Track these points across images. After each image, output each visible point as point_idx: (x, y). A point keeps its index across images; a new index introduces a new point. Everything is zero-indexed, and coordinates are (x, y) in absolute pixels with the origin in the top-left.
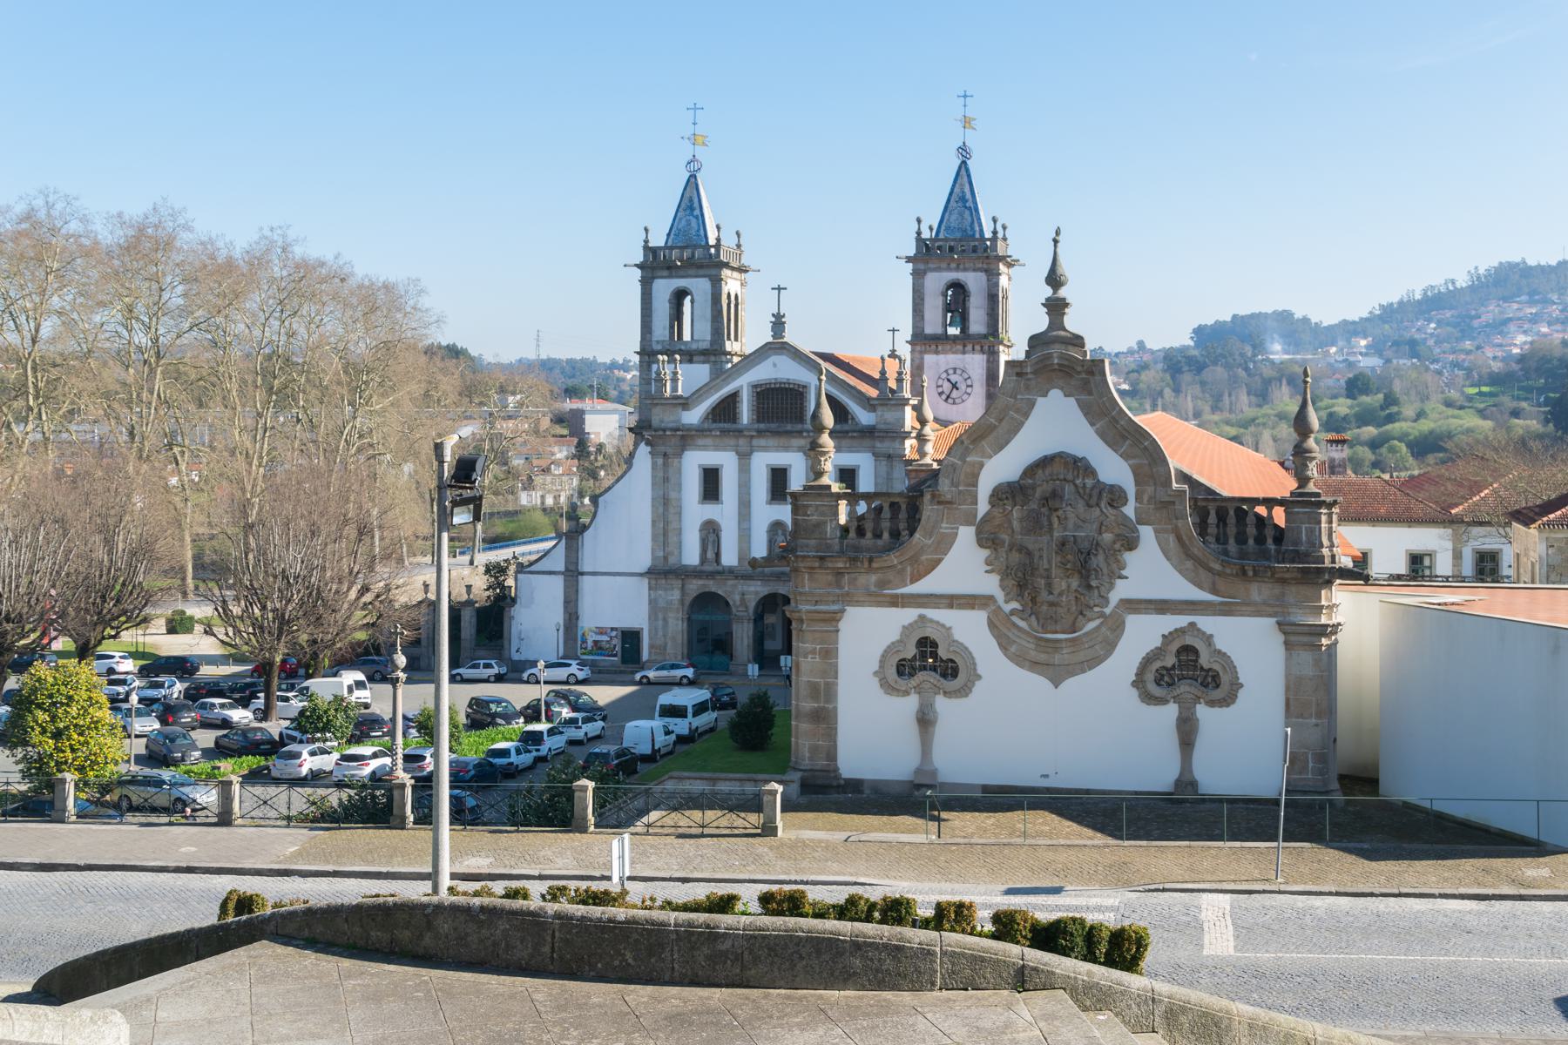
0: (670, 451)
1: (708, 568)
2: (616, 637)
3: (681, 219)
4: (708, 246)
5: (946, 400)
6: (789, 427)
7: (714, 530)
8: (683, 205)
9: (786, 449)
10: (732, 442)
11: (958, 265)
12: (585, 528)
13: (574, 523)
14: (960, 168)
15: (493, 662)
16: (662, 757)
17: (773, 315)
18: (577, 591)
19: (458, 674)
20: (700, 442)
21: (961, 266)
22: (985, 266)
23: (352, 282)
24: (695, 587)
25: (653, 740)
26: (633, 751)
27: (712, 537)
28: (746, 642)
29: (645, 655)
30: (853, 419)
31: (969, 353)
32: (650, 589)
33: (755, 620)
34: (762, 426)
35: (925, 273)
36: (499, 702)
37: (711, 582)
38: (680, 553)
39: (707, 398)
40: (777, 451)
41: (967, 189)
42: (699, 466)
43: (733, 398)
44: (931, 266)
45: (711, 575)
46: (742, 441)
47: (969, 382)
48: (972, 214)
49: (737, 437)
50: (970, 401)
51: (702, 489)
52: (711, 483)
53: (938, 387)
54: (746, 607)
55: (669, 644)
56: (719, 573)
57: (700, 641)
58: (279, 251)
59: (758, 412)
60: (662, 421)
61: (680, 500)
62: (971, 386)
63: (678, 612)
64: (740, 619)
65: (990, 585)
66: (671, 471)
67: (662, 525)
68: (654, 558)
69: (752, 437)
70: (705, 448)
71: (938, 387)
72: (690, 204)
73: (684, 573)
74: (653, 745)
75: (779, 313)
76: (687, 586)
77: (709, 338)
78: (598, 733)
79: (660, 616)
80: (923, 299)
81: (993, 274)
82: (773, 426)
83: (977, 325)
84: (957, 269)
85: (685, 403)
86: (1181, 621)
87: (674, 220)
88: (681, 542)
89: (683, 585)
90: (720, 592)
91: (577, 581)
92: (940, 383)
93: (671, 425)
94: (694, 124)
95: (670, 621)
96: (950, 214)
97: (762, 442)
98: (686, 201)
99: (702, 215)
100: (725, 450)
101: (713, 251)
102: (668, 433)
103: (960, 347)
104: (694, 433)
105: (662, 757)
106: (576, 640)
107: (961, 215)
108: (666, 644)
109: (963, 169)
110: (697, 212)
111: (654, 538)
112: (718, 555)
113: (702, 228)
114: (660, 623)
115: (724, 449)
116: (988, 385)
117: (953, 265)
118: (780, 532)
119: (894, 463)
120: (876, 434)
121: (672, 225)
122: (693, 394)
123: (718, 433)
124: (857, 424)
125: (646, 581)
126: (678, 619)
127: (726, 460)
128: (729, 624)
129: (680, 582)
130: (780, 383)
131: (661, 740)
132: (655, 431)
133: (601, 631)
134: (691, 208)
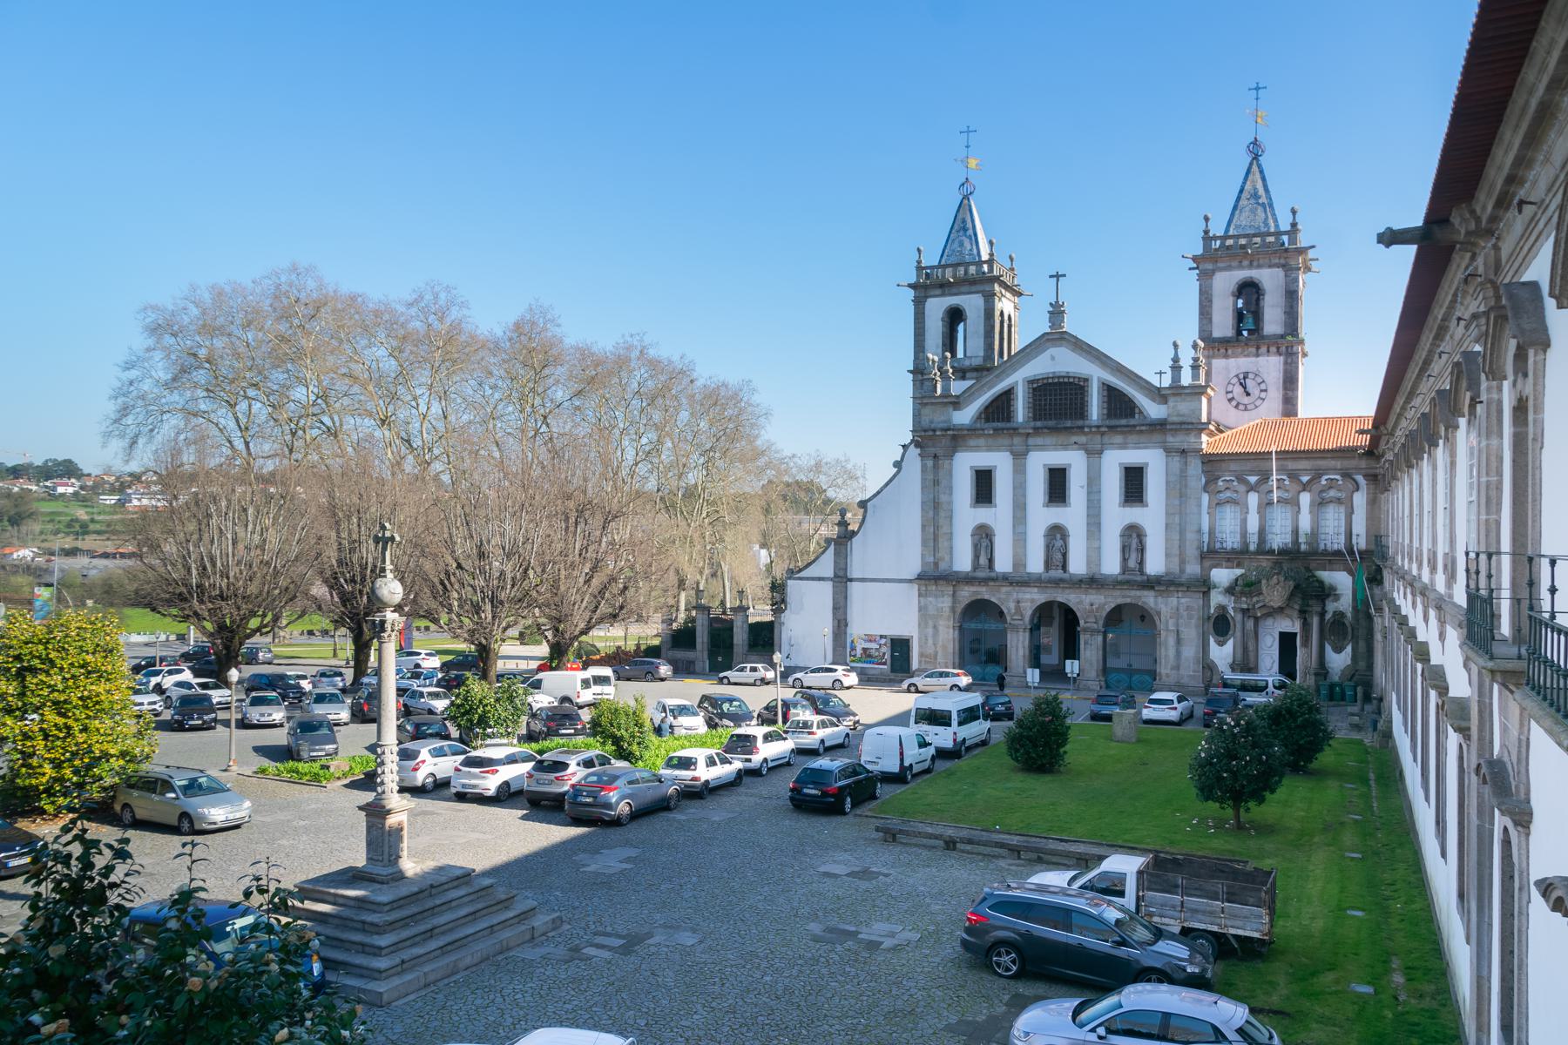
0: (940, 452)
1: (980, 574)
4: (980, 263)
5: (1236, 407)
6: (1069, 424)
7: (987, 535)
8: (956, 227)
9: (1065, 447)
10: (1006, 441)
11: (1251, 262)
12: (854, 533)
13: (843, 528)
14: (1251, 164)
15: (759, 666)
16: (914, 776)
17: (1051, 304)
18: (846, 598)
20: (972, 442)
21: (1255, 264)
22: (1282, 261)
24: (967, 594)
25: (902, 754)
26: (869, 767)
27: (985, 543)
28: (1021, 652)
29: (915, 665)
30: (1141, 412)
32: (920, 595)
33: (1031, 629)
34: (1039, 424)
35: (1213, 272)
37: (984, 589)
38: (951, 558)
39: (981, 396)
40: (1056, 450)
41: (1260, 185)
42: (971, 468)
43: (1008, 395)
44: (1221, 265)
45: (984, 581)
46: (1017, 440)
47: (1263, 386)
48: (1265, 212)
49: (1011, 436)
50: (1264, 407)
51: (974, 492)
52: (984, 486)
53: (1227, 393)
55: (940, 654)
56: (993, 579)
57: (973, 651)
60: (931, 422)
61: (950, 503)
62: (1266, 391)
63: (948, 620)
64: (1015, 628)
66: (941, 473)
68: (924, 563)
70: (977, 448)
71: (1227, 393)
72: (961, 226)
74: (902, 760)
75: (1057, 302)
76: (958, 593)
77: (982, 354)
78: (840, 741)
80: (1211, 301)
81: (1292, 269)
82: (1051, 423)
83: (1272, 323)
84: (1251, 266)
85: (957, 403)
87: (947, 241)
88: (952, 548)
89: (954, 592)
90: (993, 600)
92: (1230, 389)
94: (967, 147)
95: (941, 628)
96: (1241, 212)
97: (1039, 440)
98: (959, 221)
99: (975, 235)
100: (999, 450)
101: (985, 267)
102: (938, 433)
103: (1253, 350)
104: (966, 432)
105: (914, 776)
106: (845, 647)
107: (1253, 211)
109: (1255, 167)
110: (970, 232)
111: (924, 543)
112: (991, 561)
113: (974, 247)
114: (930, 631)
115: (998, 449)
116: (1285, 388)
117: (1246, 263)
118: (1058, 536)
119: (1189, 459)
120: (1168, 427)
121: (945, 246)
123: (991, 432)
126: (948, 627)
127: (999, 462)
128: (1003, 633)
129: (951, 588)
130: (1059, 377)
131: (913, 754)
132: (925, 431)
133: (870, 639)
134: (965, 229)
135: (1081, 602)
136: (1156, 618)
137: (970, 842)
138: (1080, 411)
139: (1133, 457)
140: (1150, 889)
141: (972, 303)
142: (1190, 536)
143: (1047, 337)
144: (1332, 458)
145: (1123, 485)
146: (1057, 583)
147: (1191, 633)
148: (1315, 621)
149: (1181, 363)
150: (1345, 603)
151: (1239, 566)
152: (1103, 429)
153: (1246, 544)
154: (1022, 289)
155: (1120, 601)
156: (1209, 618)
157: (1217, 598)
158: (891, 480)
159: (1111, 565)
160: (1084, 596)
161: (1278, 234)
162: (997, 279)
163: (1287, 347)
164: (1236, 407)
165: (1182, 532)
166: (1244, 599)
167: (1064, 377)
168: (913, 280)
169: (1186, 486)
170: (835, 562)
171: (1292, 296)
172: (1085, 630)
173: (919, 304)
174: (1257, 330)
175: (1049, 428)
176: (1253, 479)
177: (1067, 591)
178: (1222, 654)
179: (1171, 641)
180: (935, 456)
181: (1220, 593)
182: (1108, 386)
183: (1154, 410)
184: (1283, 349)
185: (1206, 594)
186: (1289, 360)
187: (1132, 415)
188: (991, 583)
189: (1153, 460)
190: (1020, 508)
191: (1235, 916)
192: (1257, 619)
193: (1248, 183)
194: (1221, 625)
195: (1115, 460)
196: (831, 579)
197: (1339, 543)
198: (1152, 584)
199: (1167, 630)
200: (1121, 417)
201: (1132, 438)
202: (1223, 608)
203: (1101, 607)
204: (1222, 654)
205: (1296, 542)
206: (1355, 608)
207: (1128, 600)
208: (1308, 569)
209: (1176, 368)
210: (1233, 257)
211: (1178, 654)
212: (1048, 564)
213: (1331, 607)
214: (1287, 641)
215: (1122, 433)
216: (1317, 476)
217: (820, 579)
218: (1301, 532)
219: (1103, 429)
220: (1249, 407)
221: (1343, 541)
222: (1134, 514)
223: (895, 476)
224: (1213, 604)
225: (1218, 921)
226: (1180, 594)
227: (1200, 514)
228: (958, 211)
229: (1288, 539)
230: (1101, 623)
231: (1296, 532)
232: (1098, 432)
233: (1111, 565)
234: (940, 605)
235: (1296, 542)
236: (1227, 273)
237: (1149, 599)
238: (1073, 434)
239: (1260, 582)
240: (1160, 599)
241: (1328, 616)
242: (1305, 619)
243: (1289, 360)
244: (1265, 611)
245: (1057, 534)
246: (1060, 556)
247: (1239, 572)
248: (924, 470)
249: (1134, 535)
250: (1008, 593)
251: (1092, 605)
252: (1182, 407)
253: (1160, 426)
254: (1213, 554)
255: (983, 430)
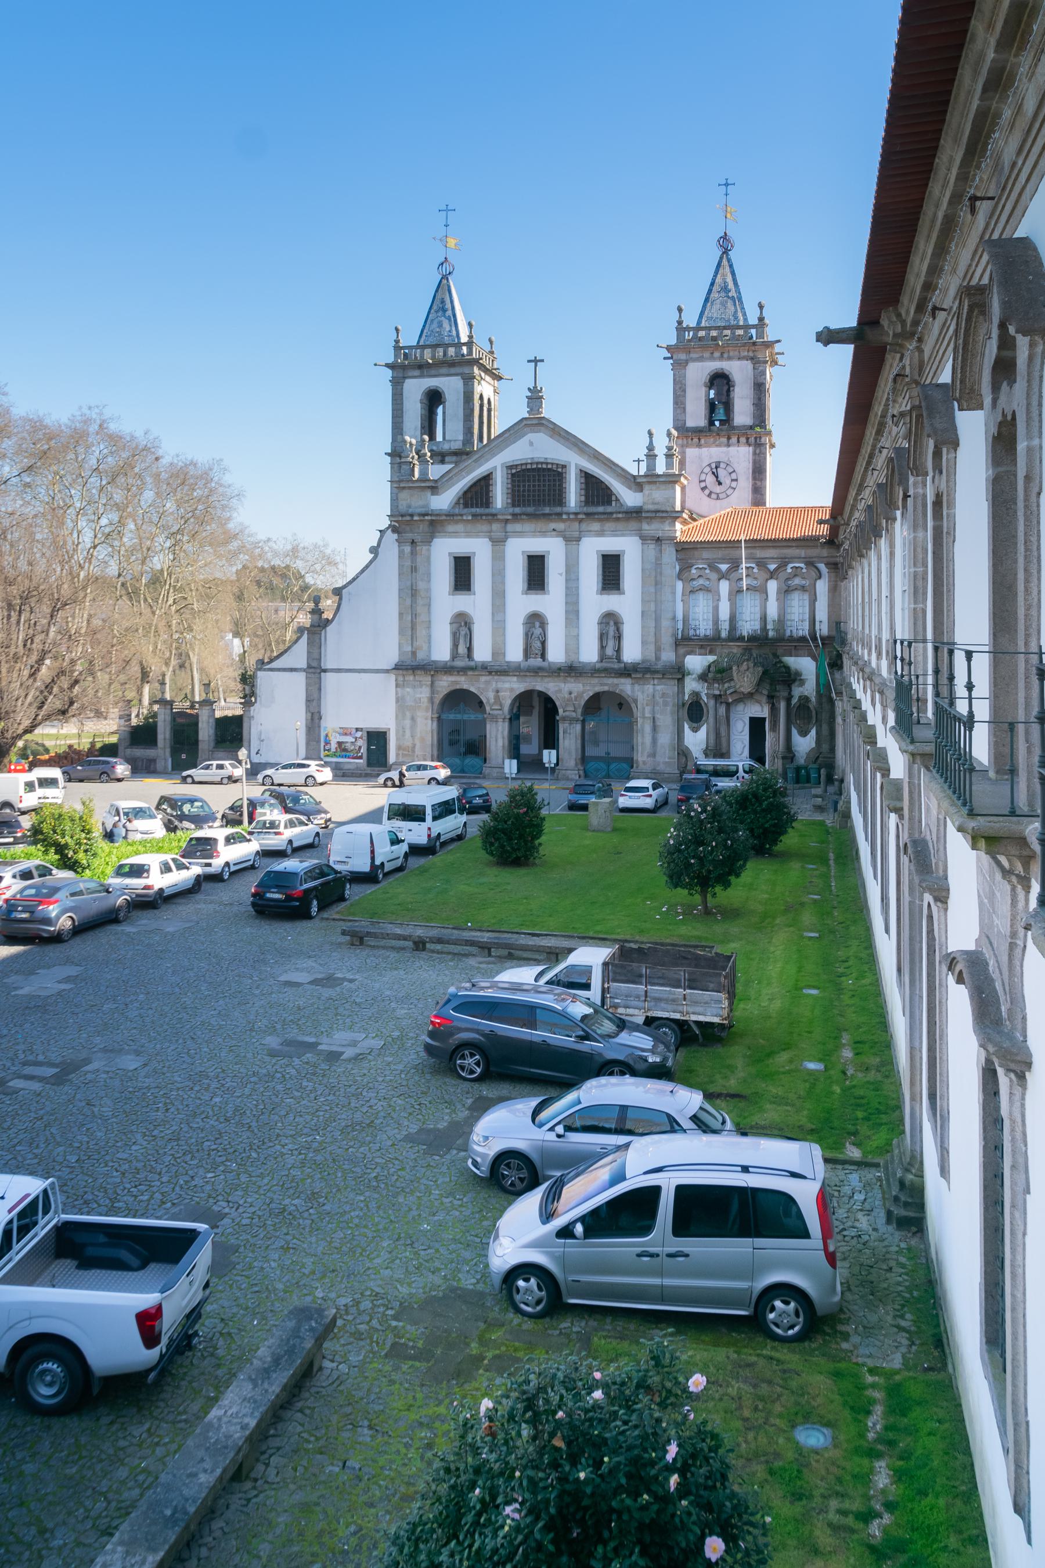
0: (418, 538)
1: (459, 663)
2: (361, 738)
3: (432, 321)
4: (459, 345)
5: (709, 496)
6: (547, 510)
7: (466, 623)
8: (435, 307)
9: (543, 534)
10: (485, 527)
11: (722, 354)
12: (328, 622)
13: (316, 617)
14: (721, 258)
16: (386, 875)
17: (529, 389)
18: (320, 689)
19: (189, 776)
20: (450, 528)
21: (726, 355)
22: (751, 354)
23: (165, 461)
24: (445, 684)
25: (373, 852)
26: (338, 867)
27: (464, 631)
28: (500, 743)
29: (392, 758)
30: (617, 500)
31: (734, 445)
32: (397, 686)
33: (510, 719)
34: (517, 510)
35: (687, 362)
36: (192, 801)
37: (463, 679)
38: (430, 647)
40: (534, 536)
41: (729, 279)
42: (450, 554)
44: (693, 355)
45: (463, 670)
46: (495, 526)
47: (734, 476)
48: (735, 305)
49: (490, 522)
50: (736, 494)
51: (453, 579)
54: (501, 705)
56: (472, 669)
57: (452, 743)
58: (97, 427)
59: (513, 496)
60: (409, 507)
61: (428, 590)
62: (736, 480)
63: (427, 711)
64: (494, 719)
66: (419, 559)
67: (410, 618)
68: (401, 653)
69: (507, 521)
70: (455, 534)
73: (432, 669)
74: (373, 859)
75: (535, 387)
76: (437, 683)
77: (461, 438)
78: (310, 840)
79: (408, 714)
80: (684, 391)
81: (759, 362)
82: (530, 510)
83: (742, 414)
84: (721, 358)
85: (434, 488)
88: (430, 636)
89: (432, 683)
90: (472, 689)
91: (320, 678)
92: (703, 477)
93: (419, 510)
94: (446, 226)
95: (419, 720)
97: (518, 527)
98: (437, 302)
99: (454, 316)
100: (478, 537)
101: (465, 350)
102: (416, 518)
103: (724, 440)
104: (444, 518)
105: (386, 875)
106: (319, 741)
107: (724, 305)
108: (414, 746)
109: (725, 262)
110: (449, 313)
112: (470, 649)
114: (408, 722)
116: (754, 478)
117: (717, 354)
118: (537, 624)
121: (424, 326)
122: (443, 476)
123: (470, 518)
124: (622, 505)
125: (392, 677)
126: (426, 719)
128: (483, 723)
129: (429, 678)
130: (537, 463)
131: (385, 852)
132: (402, 516)
133: (345, 732)
134: (444, 310)
135: (560, 691)
136: (633, 705)
137: (440, 941)
138: (558, 497)
139: (611, 544)
140: (615, 980)
141: (450, 385)
142: (665, 623)
143: (525, 422)
144: (797, 547)
145: (601, 572)
146: (536, 671)
147: (666, 720)
148: (782, 706)
149: (656, 452)
150: (809, 688)
151: (711, 653)
152: (580, 516)
153: (718, 631)
154: (502, 372)
155: (598, 689)
156: (684, 705)
157: (691, 685)
158: (367, 567)
159: (589, 654)
160: (562, 685)
161: (747, 327)
162: (476, 362)
163: (756, 438)
164: (709, 496)
165: (657, 620)
166: (716, 685)
167: (542, 463)
168: (391, 359)
169: (661, 573)
170: (309, 652)
171: (760, 389)
172: (564, 719)
173: (397, 384)
174: (727, 421)
175: (527, 515)
176: (724, 567)
177: (546, 680)
178: (696, 740)
179: (648, 728)
180: (413, 542)
181: (694, 679)
182: (586, 473)
183: (630, 498)
184: (752, 440)
185: (681, 681)
186: (758, 451)
187: (609, 503)
188: (470, 673)
190: (499, 595)
191: (696, 1003)
192: (728, 705)
193: (719, 276)
194: (695, 712)
196: (304, 670)
197: (804, 630)
198: (628, 671)
199: (644, 717)
200: (598, 504)
201: (609, 525)
202: (696, 694)
203: (580, 695)
204: (696, 740)
205: (764, 628)
206: (818, 691)
207: (606, 688)
208: (775, 655)
209: (651, 456)
210: (704, 348)
211: (654, 741)
212: (527, 652)
213: (797, 692)
214: (757, 726)
215: (600, 520)
216: (783, 565)
217: (292, 670)
218: (769, 619)
219: (580, 516)
220: (721, 496)
221: (807, 628)
222: (612, 602)
223: (371, 562)
224: (688, 690)
225: (680, 1008)
226: (656, 682)
227: (674, 601)
228: (437, 291)
229: (757, 626)
230: (580, 711)
231: (764, 619)
232: (576, 519)
233: (589, 654)
234: (418, 696)
235: (764, 628)
236: (700, 364)
237: (626, 687)
238: (551, 521)
239: (731, 668)
240: (637, 687)
241: (794, 701)
242: (773, 704)
243: (758, 451)
244: (736, 697)
245: (536, 621)
246: (539, 644)
247: (711, 658)
248: (401, 555)
249: (612, 623)
250: (487, 683)
251: (570, 693)
252: (654, 496)
253: (636, 514)
254: (686, 642)
255: (462, 515)
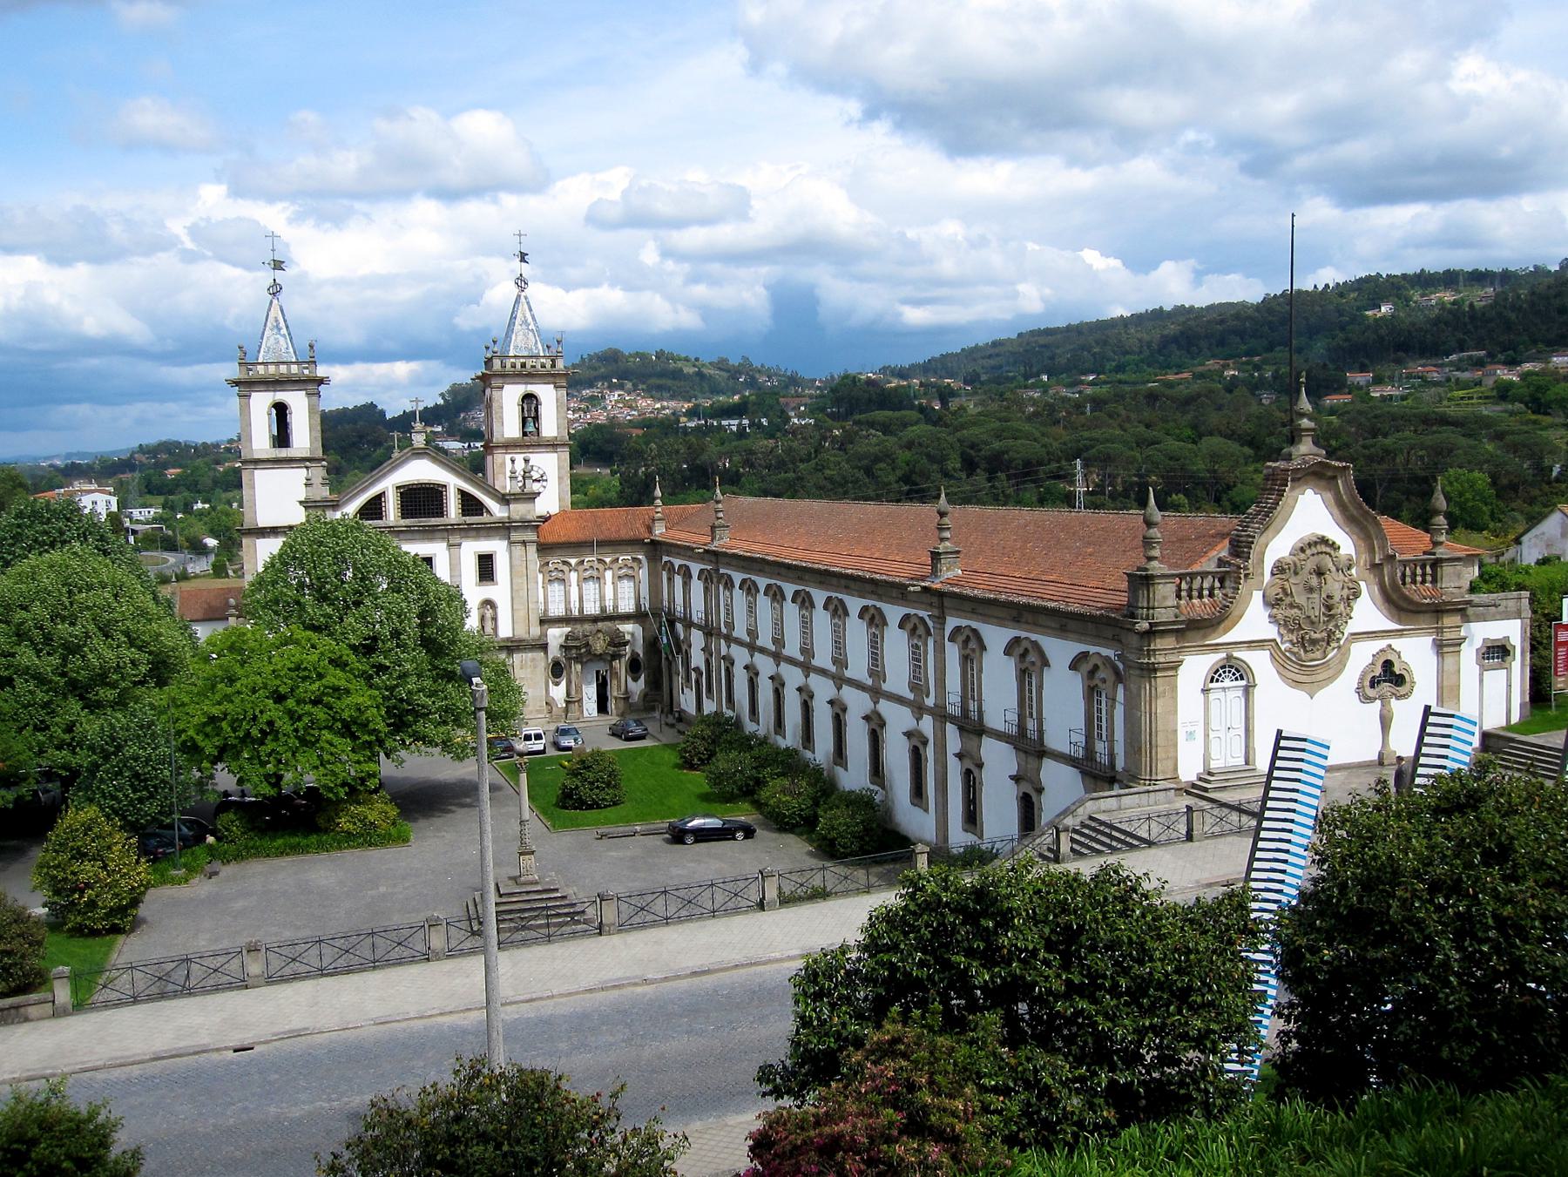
65: (1271, 632)
86: (1382, 644)
138: (439, 510)
153: (568, 609)
183: (497, 510)
189: (497, 547)
195: (471, 549)
254: (546, 621)
